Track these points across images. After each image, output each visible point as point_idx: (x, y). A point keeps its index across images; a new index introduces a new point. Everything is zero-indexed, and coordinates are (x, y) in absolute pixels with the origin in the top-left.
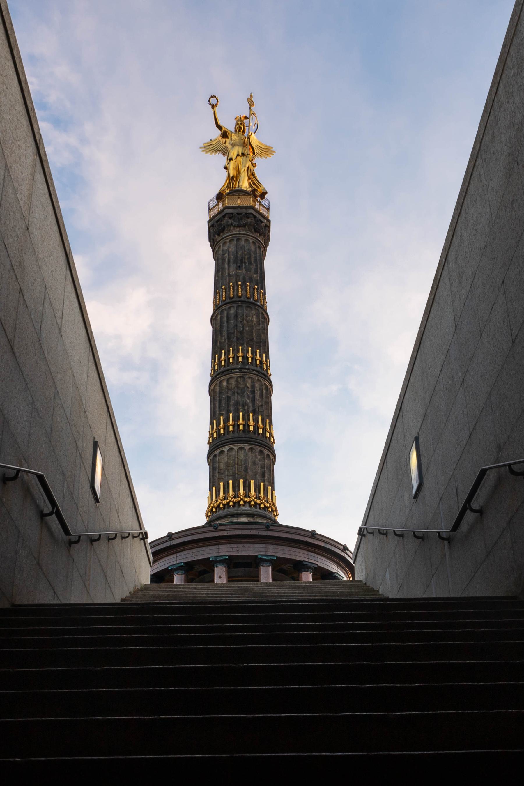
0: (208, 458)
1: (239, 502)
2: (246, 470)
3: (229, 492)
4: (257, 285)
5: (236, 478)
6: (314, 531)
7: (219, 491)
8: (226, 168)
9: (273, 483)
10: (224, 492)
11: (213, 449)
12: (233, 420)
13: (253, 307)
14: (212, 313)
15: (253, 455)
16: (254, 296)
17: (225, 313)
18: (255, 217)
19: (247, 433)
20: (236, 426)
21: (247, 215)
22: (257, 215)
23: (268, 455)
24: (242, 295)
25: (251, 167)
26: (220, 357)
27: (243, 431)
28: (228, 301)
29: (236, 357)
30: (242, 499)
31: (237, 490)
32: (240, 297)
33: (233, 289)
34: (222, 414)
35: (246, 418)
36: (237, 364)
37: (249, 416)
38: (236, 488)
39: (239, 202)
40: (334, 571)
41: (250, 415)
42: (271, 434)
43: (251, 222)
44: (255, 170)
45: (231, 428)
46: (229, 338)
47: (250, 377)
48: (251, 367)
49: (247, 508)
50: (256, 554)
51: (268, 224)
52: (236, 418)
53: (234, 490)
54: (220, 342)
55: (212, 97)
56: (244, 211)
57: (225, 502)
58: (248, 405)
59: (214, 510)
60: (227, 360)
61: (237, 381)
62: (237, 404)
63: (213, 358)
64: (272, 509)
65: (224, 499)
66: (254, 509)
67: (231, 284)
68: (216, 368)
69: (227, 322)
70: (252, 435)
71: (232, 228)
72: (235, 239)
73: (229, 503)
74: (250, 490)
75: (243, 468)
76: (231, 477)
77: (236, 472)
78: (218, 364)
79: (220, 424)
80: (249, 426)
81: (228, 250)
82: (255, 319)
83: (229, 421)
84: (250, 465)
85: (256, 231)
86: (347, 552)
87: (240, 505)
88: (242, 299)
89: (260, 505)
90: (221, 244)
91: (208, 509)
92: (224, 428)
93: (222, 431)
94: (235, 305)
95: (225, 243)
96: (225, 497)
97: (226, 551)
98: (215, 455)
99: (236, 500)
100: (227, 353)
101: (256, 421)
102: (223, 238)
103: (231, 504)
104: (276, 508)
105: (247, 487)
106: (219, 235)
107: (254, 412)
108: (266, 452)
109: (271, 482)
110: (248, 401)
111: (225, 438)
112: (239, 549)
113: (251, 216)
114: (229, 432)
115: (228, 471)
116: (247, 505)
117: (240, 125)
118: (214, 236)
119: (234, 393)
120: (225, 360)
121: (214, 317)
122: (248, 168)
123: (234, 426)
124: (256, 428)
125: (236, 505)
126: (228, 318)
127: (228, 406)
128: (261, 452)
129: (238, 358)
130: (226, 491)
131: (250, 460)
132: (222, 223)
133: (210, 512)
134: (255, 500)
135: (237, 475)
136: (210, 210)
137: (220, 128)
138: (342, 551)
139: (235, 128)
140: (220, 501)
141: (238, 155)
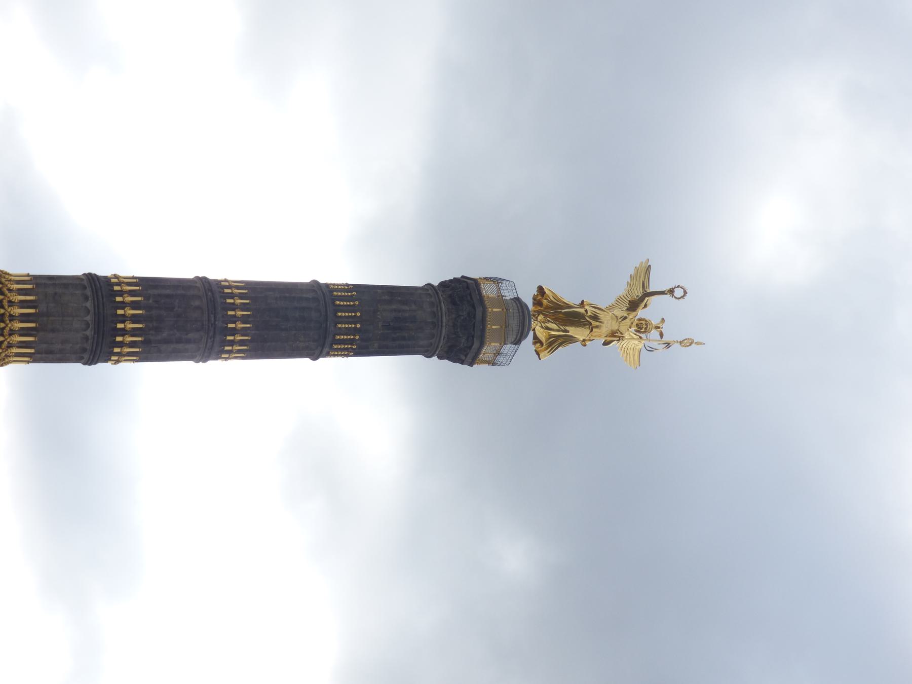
2: (53, 331)
10: (21, 301)
12: (133, 315)
18: (470, 348)
26: (241, 296)
27: (116, 329)
30: (7, 325)
34: (147, 298)
38: (24, 318)
45: (120, 312)
52: (135, 319)
57: (5, 303)
71: (454, 316)
74: (21, 335)
77: (51, 318)
90: (433, 299)
95: (432, 304)
98: (85, 288)
102: (440, 302)
106: (450, 296)
120: (233, 304)
123: (123, 315)
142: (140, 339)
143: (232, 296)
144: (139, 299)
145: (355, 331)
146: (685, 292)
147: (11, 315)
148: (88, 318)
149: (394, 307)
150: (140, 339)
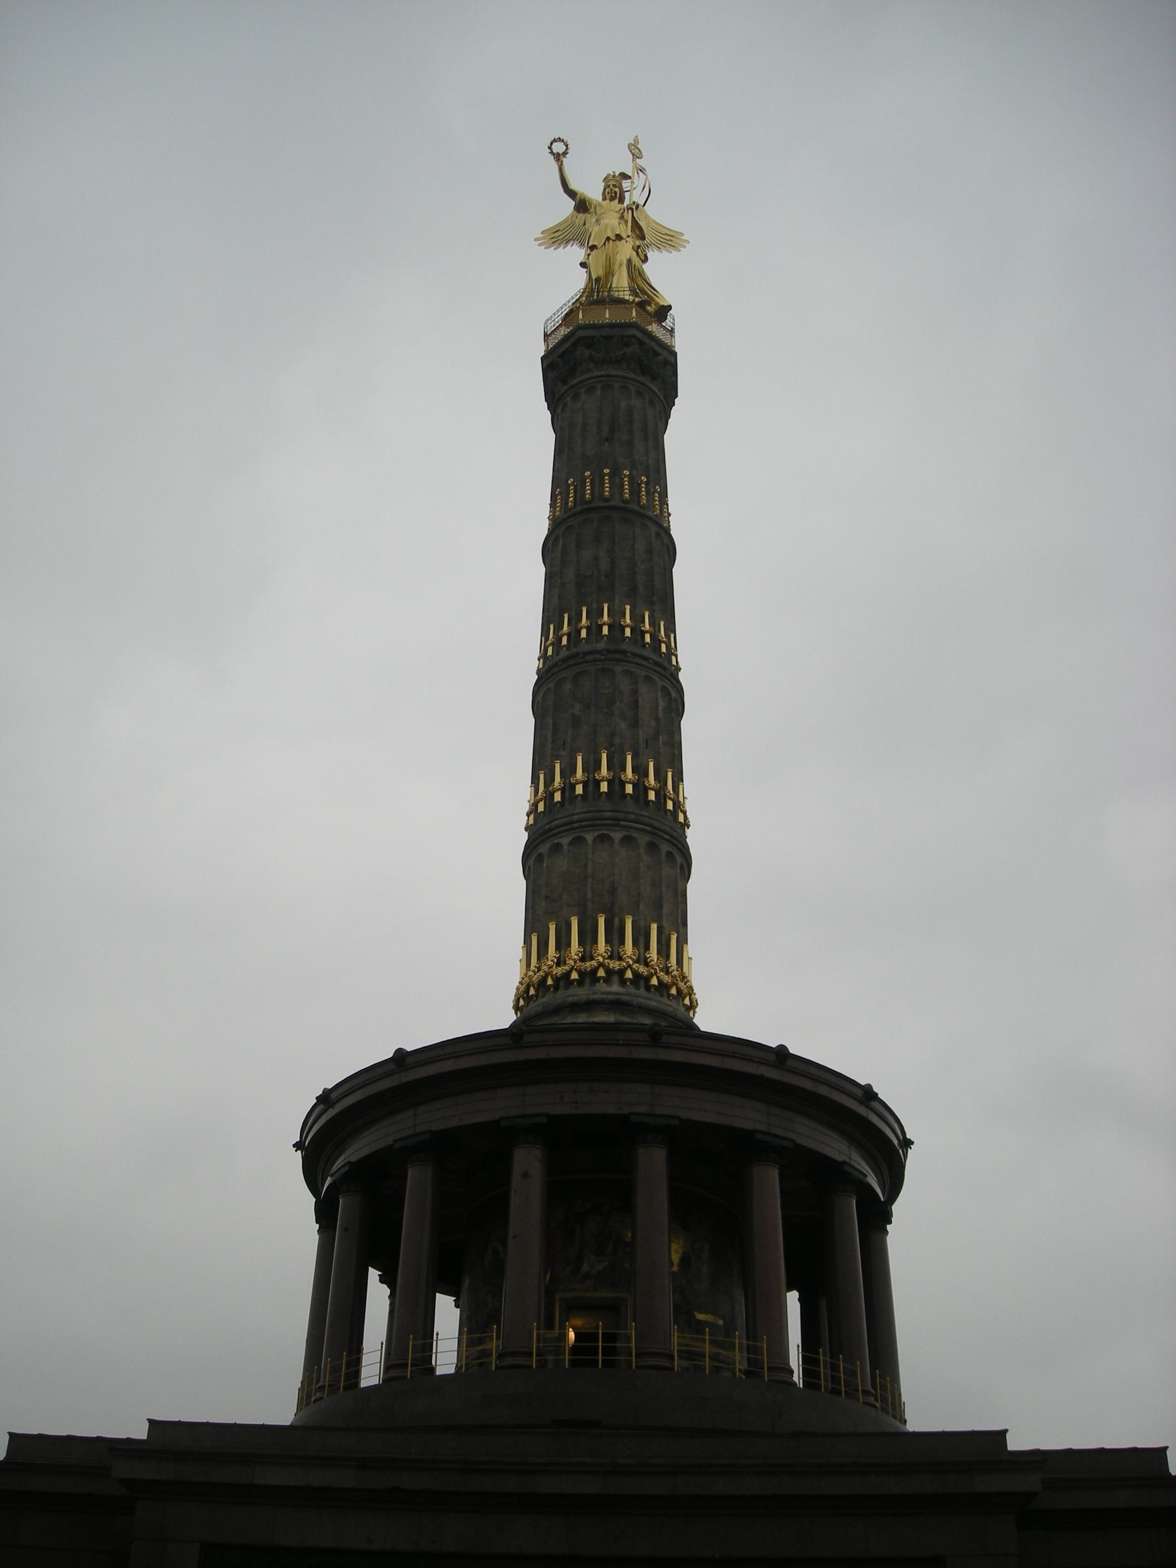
2: (613, 891)
3: (569, 945)
6: (782, 1049)
8: (583, 265)
9: (685, 924)
10: (558, 948)
11: (534, 841)
16: (639, 497)
18: (641, 343)
20: (592, 784)
22: (646, 340)
28: (579, 508)
30: (601, 965)
32: (606, 500)
33: (592, 482)
34: (557, 757)
35: (616, 766)
38: (588, 936)
39: (607, 316)
40: (840, 1158)
42: (679, 806)
44: (646, 267)
45: (579, 789)
47: (626, 672)
49: (615, 987)
50: (625, 1111)
51: (673, 360)
52: (592, 766)
55: (555, 140)
57: (559, 971)
59: (532, 992)
60: (574, 635)
63: (545, 632)
64: (679, 991)
65: (558, 964)
66: (632, 990)
68: (550, 652)
71: (592, 365)
72: (599, 387)
73: (569, 973)
74: (622, 942)
77: (589, 895)
78: (552, 644)
79: (553, 780)
80: (623, 784)
83: (574, 771)
85: (645, 370)
86: (875, 1104)
87: (597, 980)
88: (612, 503)
89: (647, 979)
91: (518, 989)
92: (563, 790)
93: (558, 797)
95: (576, 397)
96: (558, 959)
98: (540, 856)
100: (575, 619)
102: (573, 386)
104: (691, 988)
105: (615, 935)
106: (564, 382)
109: (680, 922)
116: (615, 979)
117: (614, 188)
120: (569, 635)
121: (550, 545)
122: (629, 261)
123: (585, 784)
124: (641, 788)
125: (588, 981)
129: (600, 627)
130: (563, 943)
133: (523, 999)
134: (635, 966)
135: (589, 904)
136: (546, 336)
137: (571, 194)
138: (861, 1103)
139: (604, 194)
140: (545, 968)
141: (608, 239)
142: (629, 758)
144: (558, 766)
145: (616, 474)
146: (560, 140)
147: (583, 959)
148: (589, 837)
150: (629, 758)
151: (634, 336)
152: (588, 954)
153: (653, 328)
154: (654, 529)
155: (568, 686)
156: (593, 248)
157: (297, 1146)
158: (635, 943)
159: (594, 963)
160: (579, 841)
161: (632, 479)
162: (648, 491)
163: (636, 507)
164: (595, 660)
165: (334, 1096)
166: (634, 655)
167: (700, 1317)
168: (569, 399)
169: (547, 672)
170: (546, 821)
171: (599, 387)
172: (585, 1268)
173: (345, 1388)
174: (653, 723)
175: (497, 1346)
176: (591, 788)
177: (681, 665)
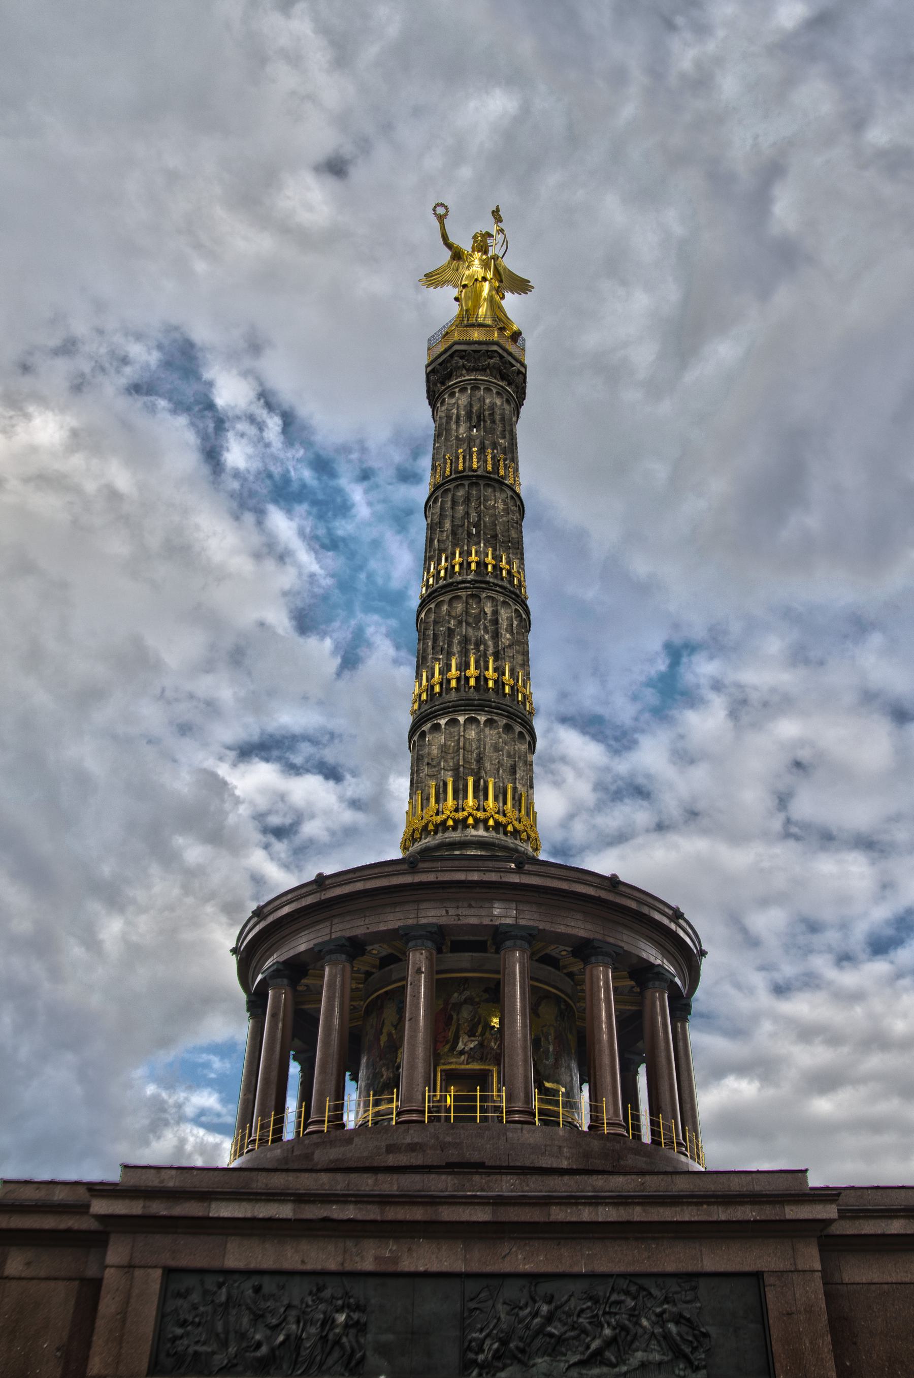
0: (411, 737)
1: (466, 819)
2: (479, 760)
3: (445, 800)
4: (505, 454)
5: (461, 774)
7: (428, 799)
8: (457, 299)
11: (420, 720)
13: (496, 485)
14: (427, 496)
15: (494, 732)
17: (450, 496)
18: (501, 357)
19: (482, 691)
21: (490, 354)
22: (505, 355)
23: (520, 733)
24: (478, 467)
25: (498, 298)
27: (477, 688)
28: (453, 476)
29: (465, 563)
30: (470, 814)
31: (461, 796)
32: (475, 471)
33: (464, 458)
34: (439, 660)
35: (481, 664)
36: (467, 575)
37: (486, 663)
38: (461, 793)
41: (488, 662)
43: (495, 363)
45: (453, 683)
46: (454, 533)
47: (488, 597)
48: (491, 580)
49: (481, 832)
51: (523, 370)
53: (455, 797)
54: (438, 541)
56: (484, 348)
57: (439, 819)
58: (485, 645)
60: (450, 570)
61: (467, 603)
62: (465, 640)
65: (437, 814)
66: (493, 834)
67: (461, 451)
69: (452, 508)
70: (492, 696)
71: (464, 372)
72: (469, 387)
74: (486, 798)
75: (475, 755)
76: (450, 773)
77: (461, 763)
80: (486, 680)
81: (457, 403)
82: (501, 506)
83: (449, 670)
84: (489, 751)
85: (503, 378)
88: (479, 473)
92: (441, 684)
93: (437, 689)
94: (466, 483)
95: (452, 395)
97: (432, 915)
99: (461, 815)
101: (499, 670)
102: (450, 386)
103: (450, 822)
105: (481, 791)
106: (443, 383)
107: (497, 656)
108: (518, 729)
110: (486, 637)
111: (441, 701)
112: (460, 912)
113: (496, 354)
114: (449, 689)
115: (446, 761)
116: (481, 826)
117: (482, 243)
118: (435, 384)
119: (460, 622)
120: (446, 569)
123: (458, 679)
125: (460, 827)
126: (454, 503)
127: (450, 645)
128: (508, 728)
129: (469, 564)
131: (489, 742)
132: (449, 365)
134: (496, 816)
135: (461, 769)
136: (429, 349)
137: (449, 246)
138: (671, 920)
140: (426, 817)
143: (437, 576)
147: (456, 810)
148: (461, 719)
149: (454, 427)
151: (496, 351)
152: (460, 806)
153: (511, 348)
154: (510, 493)
155: (445, 607)
156: (465, 286)
157: (234, 951)
158: (496, 798)
159: (466, 813)
160: (453, 722)
161: (493, 458)
162: (505, 465)
163: (496, 477)
164: (466, 588)
165: (266, 910)
166: (497, 585)
167: (548, 1085)
168: (446, 396)
169: (429, 596)
170: (427, 707)
171: (469, 387)
172: (460, 1046)
173: (273, 1141)
174: (508, 636)
175: (397, 1107)
176: (463, 683)
177: (528, 594)
